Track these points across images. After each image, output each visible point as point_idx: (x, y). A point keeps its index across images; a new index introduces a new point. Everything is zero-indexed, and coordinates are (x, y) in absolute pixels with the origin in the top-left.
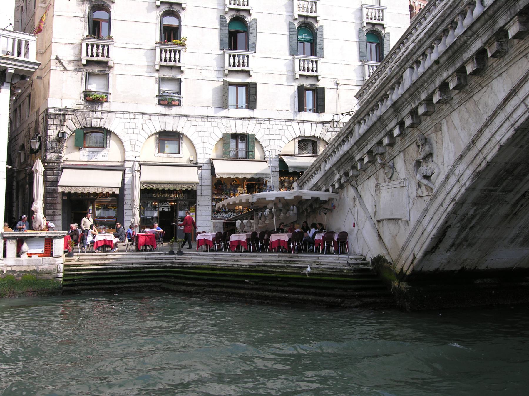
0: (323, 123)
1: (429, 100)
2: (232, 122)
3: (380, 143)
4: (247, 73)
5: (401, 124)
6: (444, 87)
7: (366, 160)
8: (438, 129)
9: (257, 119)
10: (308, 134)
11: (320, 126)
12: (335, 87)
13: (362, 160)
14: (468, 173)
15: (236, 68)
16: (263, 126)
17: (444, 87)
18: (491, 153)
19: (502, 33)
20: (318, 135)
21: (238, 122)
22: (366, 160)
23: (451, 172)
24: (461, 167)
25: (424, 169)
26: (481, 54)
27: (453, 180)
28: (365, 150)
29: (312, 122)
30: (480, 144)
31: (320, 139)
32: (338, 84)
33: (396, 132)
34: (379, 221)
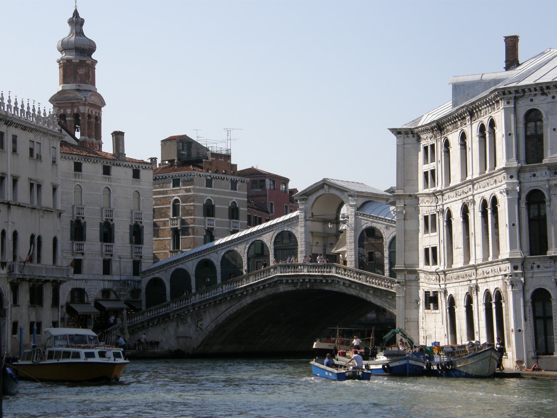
0: (114, 281)
1: (205, 305)
2: (75, 281)
3: (184, 312)
4: (83, 254)
5: (194, 309)
6: (210, 303)
7: (176, 316)
8: (205, 312)
9: (85, 280)
10: (107, 288)
11: (112, 282)
12: (119, 260)
13: (173, 316)
14: (214, 326)
15: (78, 252)
16: (88, 284)
17: (210, 303)
18: (220, 322)
19: (226, 298)
20: (111, 288)
21: (78, 282)
22: (176, 316)
23: (209, 325)
24: (212, 324)
25: (200, 323)
26: (221, 300)
27: (209, 327)
28: (176, 313)
29: (108, 281)
30: (218, 319)
31: (111, 290)
32: (120, 258)
33: (191, 311)
34: (177, 338)
